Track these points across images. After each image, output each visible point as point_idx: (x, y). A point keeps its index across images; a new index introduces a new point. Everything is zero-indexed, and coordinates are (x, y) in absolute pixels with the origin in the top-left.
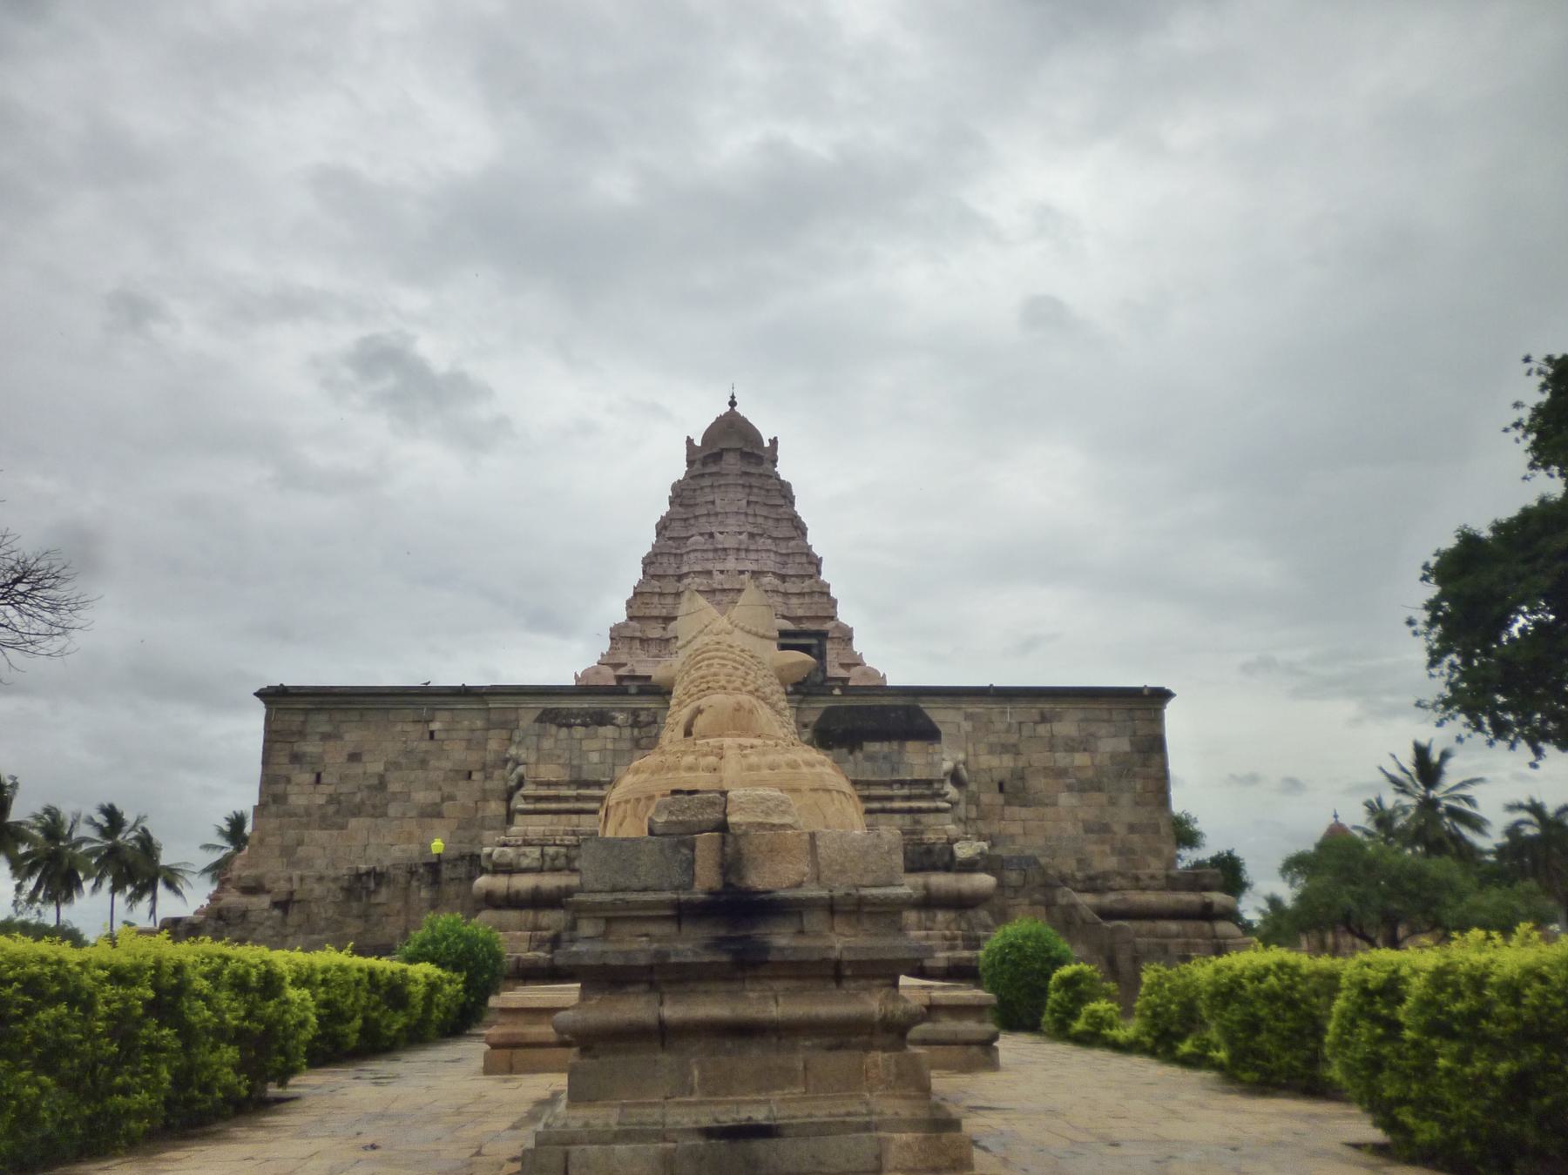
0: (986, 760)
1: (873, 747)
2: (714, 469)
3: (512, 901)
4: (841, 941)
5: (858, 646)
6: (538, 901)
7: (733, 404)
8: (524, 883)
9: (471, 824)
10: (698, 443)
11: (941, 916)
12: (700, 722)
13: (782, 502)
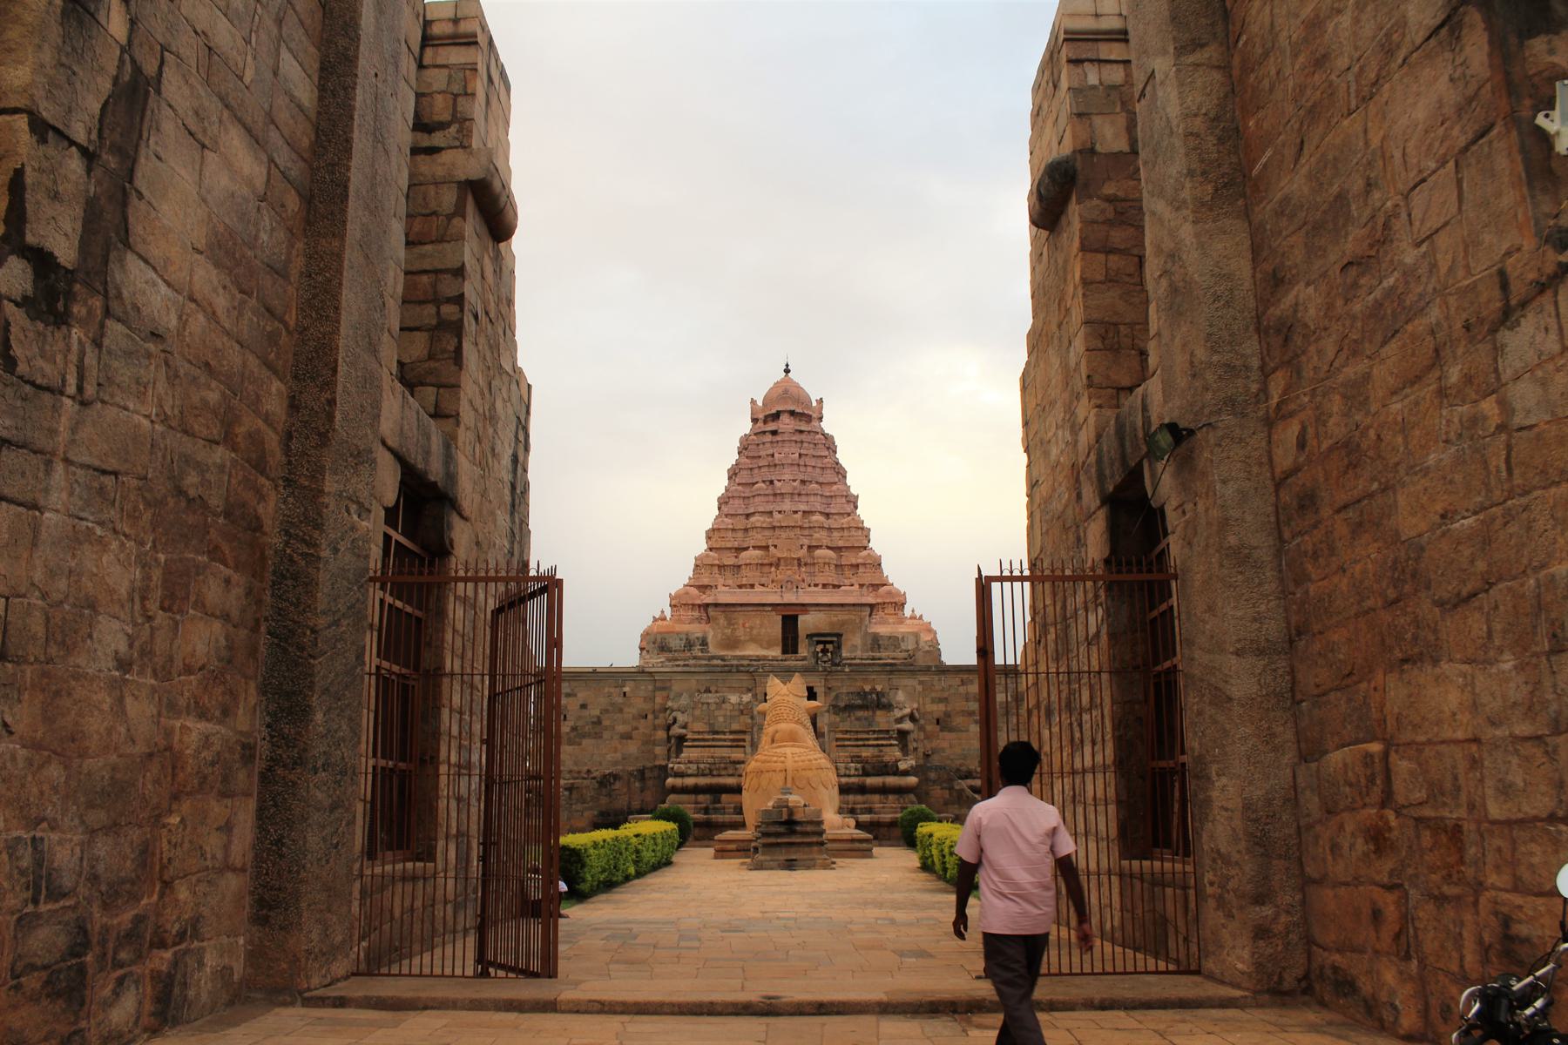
0: (931, 707)
1: (860, 714)
2: (772, 426)
3: (684, 790)
4: (809, 828)
5: (888, 569)
6: (696, 790)
7: (787, 371)
8: (690, 781)
9: (649, 742)
10: (760, 403)
11: (891, 797)
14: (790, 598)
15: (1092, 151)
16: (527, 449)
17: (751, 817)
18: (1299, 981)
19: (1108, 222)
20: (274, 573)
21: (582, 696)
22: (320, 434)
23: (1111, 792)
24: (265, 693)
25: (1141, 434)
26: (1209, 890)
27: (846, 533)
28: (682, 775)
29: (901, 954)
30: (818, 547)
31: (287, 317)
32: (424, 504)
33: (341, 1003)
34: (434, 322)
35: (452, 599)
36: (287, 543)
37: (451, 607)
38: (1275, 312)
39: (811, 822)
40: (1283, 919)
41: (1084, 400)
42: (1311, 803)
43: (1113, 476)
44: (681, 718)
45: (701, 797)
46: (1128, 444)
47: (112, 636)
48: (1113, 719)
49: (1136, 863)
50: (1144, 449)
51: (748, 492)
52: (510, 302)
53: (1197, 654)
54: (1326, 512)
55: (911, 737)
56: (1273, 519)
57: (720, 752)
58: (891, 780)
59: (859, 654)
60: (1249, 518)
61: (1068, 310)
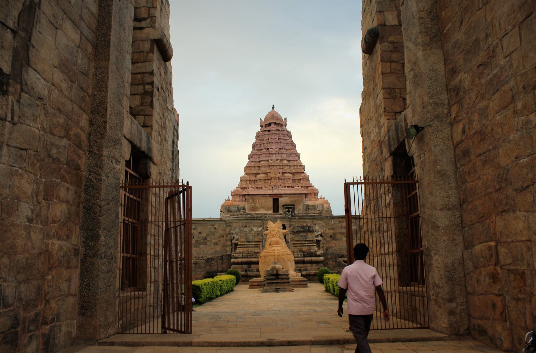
0: (328, 231)
1: (302, 234)
2: (268, 128)
4: (284, 277)
6: (242, 263)
7: (273, 108)
8: (240, 260)
9: (224, 246)
10: (263, 120)
11: (314, 265)
12: (272, 243)
13: (288, 138)
14: (276, 192)
15: (385, 25)
16: (178, 138)
17: (262, 273)
18: (466, 330)
19: (391, 51)
20: (85, 185)
21: (199, 229)
22: (101, 134)
23: (395, 261)
24: (82, 230)
25: (404, 129)
26: (432, 297)
27: (296, 167)
28: (237, 258)
29: (319, 323)
30: (286, 173)
31: (88, 91)
32: (140, 159)
33: (112, 344)
34: (143, 92)
35: (151, 194)
36: (90, 174)
37: (150, 197)
38: (453, 83)
39: (285, 275)
40: (459, 307)
41: (383, 117)
42: (469, 265)
43: (394, 144)
44: (236, 237)
45: (244, 266)
46: (399, 133)
47: (26, 209)
48: (395, 235)
49: (405, 288)
50: (405, 135)
51: (259, 153)
52: (171, 84)
53: (426, 210)
54: (473, 157)
55: (321, 242)
56: (453, 160)
57: (250, 249)
58: (314, 259)
59: (301, 212)
60: (444, 159)
61: (376, 84)
